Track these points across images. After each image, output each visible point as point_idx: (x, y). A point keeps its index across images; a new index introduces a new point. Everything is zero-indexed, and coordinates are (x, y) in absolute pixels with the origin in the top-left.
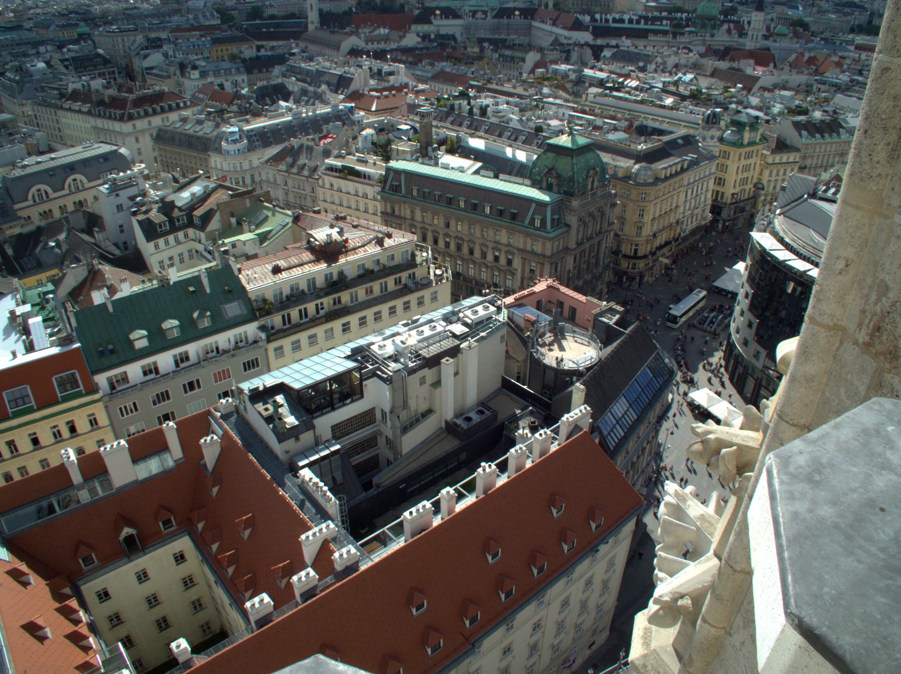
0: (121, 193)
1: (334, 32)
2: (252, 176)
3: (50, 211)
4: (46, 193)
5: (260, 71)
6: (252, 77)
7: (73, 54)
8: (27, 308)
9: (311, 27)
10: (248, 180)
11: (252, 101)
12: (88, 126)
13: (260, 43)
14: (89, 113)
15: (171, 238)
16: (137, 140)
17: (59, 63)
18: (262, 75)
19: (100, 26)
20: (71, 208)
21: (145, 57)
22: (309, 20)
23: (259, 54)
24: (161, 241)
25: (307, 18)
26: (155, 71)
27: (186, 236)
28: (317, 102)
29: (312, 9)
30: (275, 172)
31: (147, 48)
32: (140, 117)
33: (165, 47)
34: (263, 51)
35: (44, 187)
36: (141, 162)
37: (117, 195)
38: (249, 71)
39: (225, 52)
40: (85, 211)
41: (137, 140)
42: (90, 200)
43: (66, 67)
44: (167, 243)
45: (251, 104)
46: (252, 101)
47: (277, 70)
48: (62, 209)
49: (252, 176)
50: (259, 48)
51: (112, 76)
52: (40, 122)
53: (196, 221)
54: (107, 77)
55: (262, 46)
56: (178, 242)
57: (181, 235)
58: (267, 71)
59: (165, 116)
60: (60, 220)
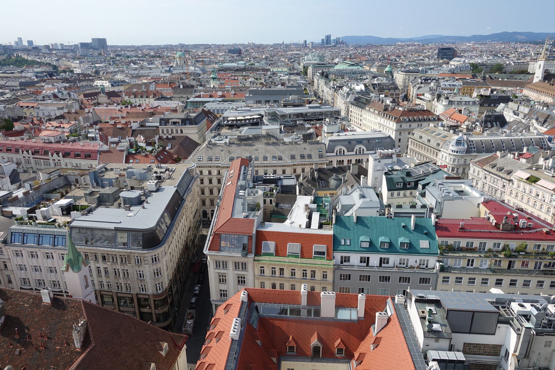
0: (382, 160)
1: (553, 85)
2: (464, 169)
3: (343, 161)
4: (344, 151)
5: (489, 106)
6: (482, 108)
7: (379, 82)
8: (314, 206)
9: (536, 80)
10: (460, 171)
11: (477, 123)
12: (376, 121)
13: (494, 88)
14: (379, 114)
15: (402, 192)
16: (400, 134)
17: (371, 85)
18: (489, 108)
19: (399, 68)
20: (354, 162)
21: (419, 88)
22: (535, 76)
23: (492, 94)
24: (396, 193)
25: (534, 74)
26: (422, 97)
27: (411, 193)
28: (524, 131)
29: (540, 68)
30: (480, 170)
31: (421, 83)
32: (405, 121)
33: (432, 84)
34: (495, 93)
35: (343, 148)
36: (399, 146)
37: (379, 161)
38: (481, 105)
39: (469, 91)
40: (360, 165)
41: (400, 134)
42: (365, 160)
43: (374, 88)
44: (399, 194)
45: (477, 125)
46: (477, 123)
47: (502, 105)
48: (350, 161)
49: (464, 169)
50: (492, 91)
51: (397, 96)
52: (352, 114)
53: (420, 187)
54: (394, 96)
55: (495, 90)
56: (405, 196)
57: (408, 192)
58: (495, 106)
59: (420, 123)
60: (346, 167)
